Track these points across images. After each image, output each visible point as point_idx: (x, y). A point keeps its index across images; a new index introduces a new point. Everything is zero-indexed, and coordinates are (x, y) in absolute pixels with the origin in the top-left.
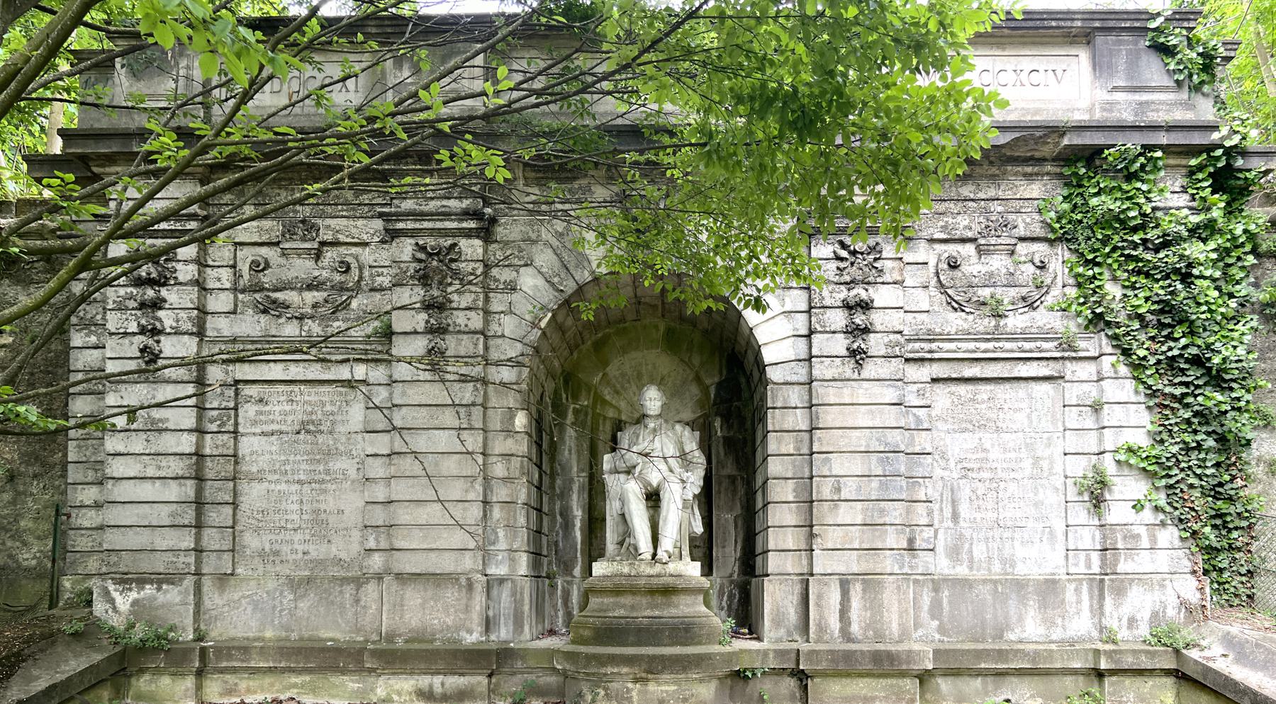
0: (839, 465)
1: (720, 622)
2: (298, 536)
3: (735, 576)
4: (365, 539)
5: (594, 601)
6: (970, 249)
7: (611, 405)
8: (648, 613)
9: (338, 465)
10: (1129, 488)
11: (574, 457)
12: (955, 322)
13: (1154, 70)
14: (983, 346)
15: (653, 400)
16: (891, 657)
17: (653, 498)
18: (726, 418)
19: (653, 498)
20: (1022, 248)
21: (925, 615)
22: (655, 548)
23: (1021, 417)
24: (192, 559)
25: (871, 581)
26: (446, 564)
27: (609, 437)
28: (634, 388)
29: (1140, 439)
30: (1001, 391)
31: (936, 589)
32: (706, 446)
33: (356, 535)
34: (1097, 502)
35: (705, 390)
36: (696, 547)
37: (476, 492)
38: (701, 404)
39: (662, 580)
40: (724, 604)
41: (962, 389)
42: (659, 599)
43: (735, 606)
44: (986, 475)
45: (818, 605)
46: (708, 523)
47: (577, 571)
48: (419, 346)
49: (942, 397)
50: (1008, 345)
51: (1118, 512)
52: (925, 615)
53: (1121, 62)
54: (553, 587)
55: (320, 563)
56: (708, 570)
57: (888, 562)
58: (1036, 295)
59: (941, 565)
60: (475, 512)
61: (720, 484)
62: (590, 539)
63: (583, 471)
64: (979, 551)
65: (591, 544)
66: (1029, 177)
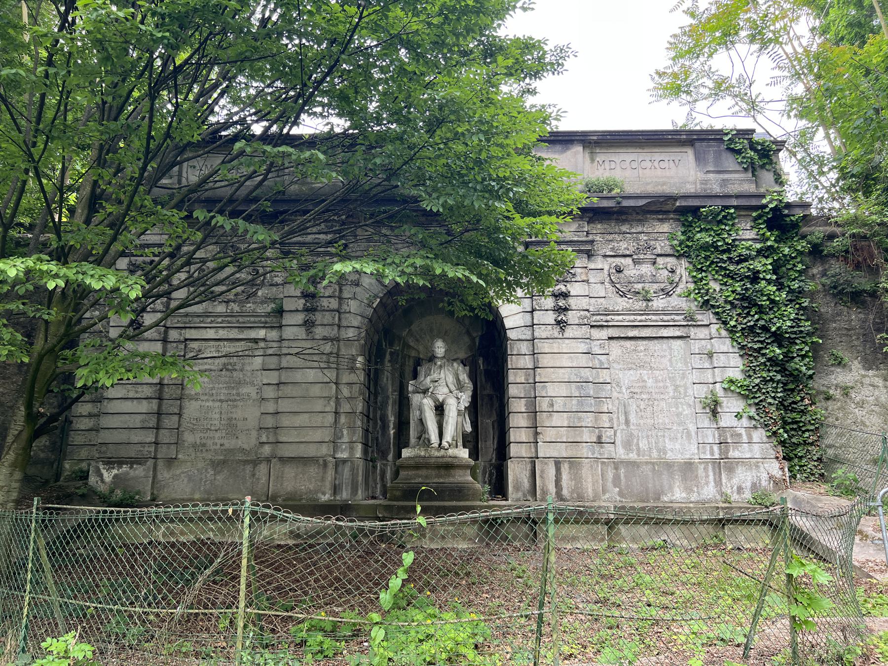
1: (482, 487)
2: (218, 435)
3: (494, 461)
5: (403, 473)
6: (629, 261)
7: (414, 349)
8: (436, 480)
9: (244, 390)
10: (732, 405)
11: (390, 382)
12: (622, 303)
13: (730, 162)
14: (639, 318)
15: (440, 348)
17: (440, 409)
18: (486, 360)
19: (440, 409)
20: (660, 260)
21: (610, 485)
22: (441, 440)
23: (665, 361)
24: (152, 449)
25: (574, 462)
26: (311, 451)
28: (428, 337)
30: (654, 345)
31: (616, 468)
32: (473, 376)
33: (254, 434)
34: (714, 413)
36: (468, 441)
39: (445, 460)
40: (486, 479)
41: (628, 344)
42: (443, 472)
43: (493, 481)
44: (644, 396)
45: (541, 477)
46: (475, 424)
47: (390, 457)
48: (300, 318)
49: (616, 349)
50: (654, 318)
51: (727, 420)
52: (610, 485)
53: (711, 157)
54: (375, 467)
55: (231, 451)
56: (474, 454)
57: (585, 450)
58: (669, 288)
59: (620, 453)
60: (330, 418)
61: (482, 400)
62: (399, 436)
63: (395, 391)
64: (643, 444)
65: (399, 439)
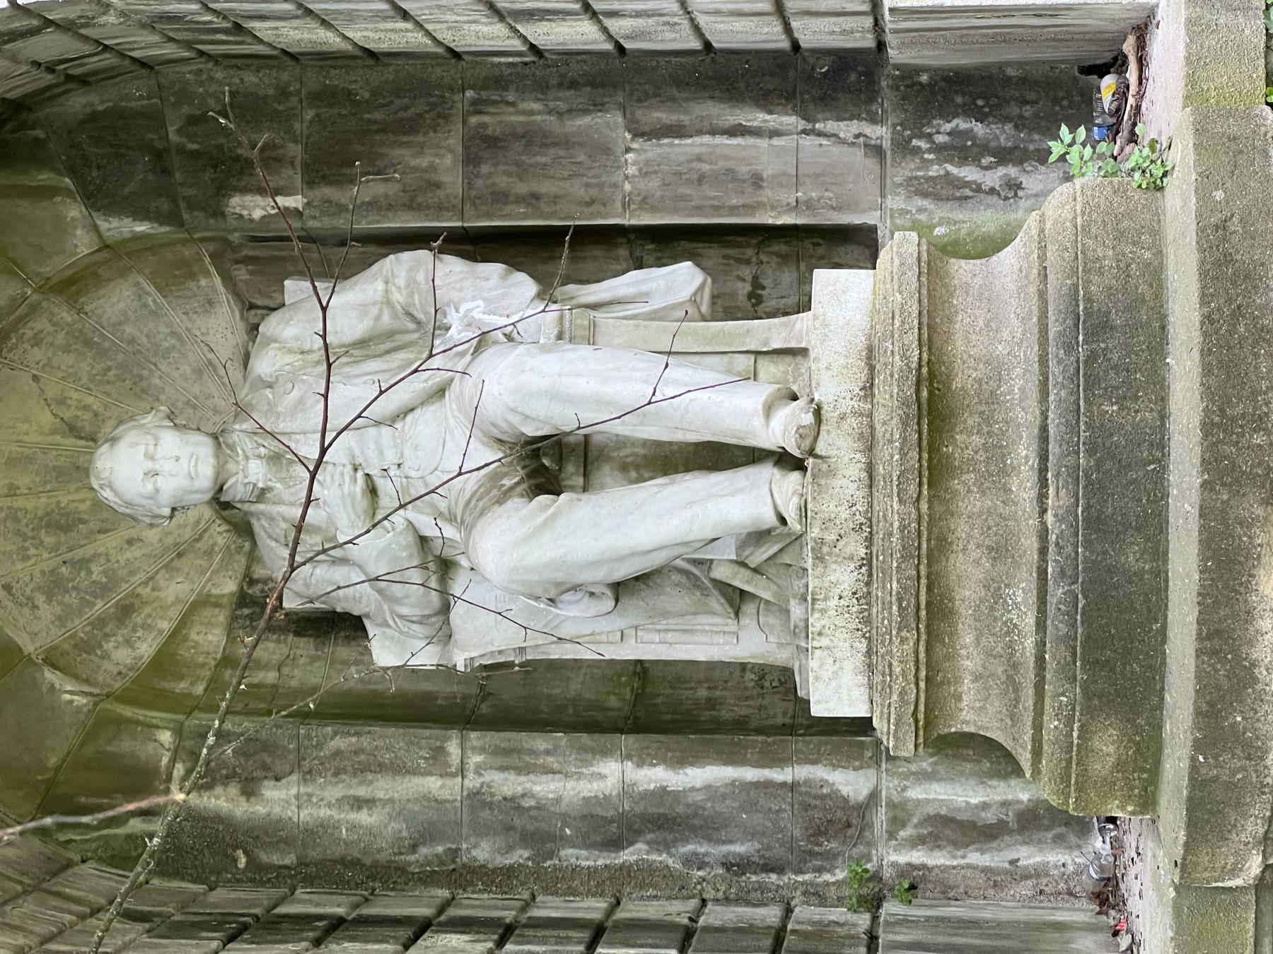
3: (880, 133)
15: (151, 466)
17: (550, 463)
27: (305, 647)
32: (342, 253)
35: (116, 258)
38: (174, 276)
40: (992, 178)
43: (1004, 134)
47: (851, 782)
61: (500, 198)
62: (718, 727)
63: (439, 753)
65: (740, 726)
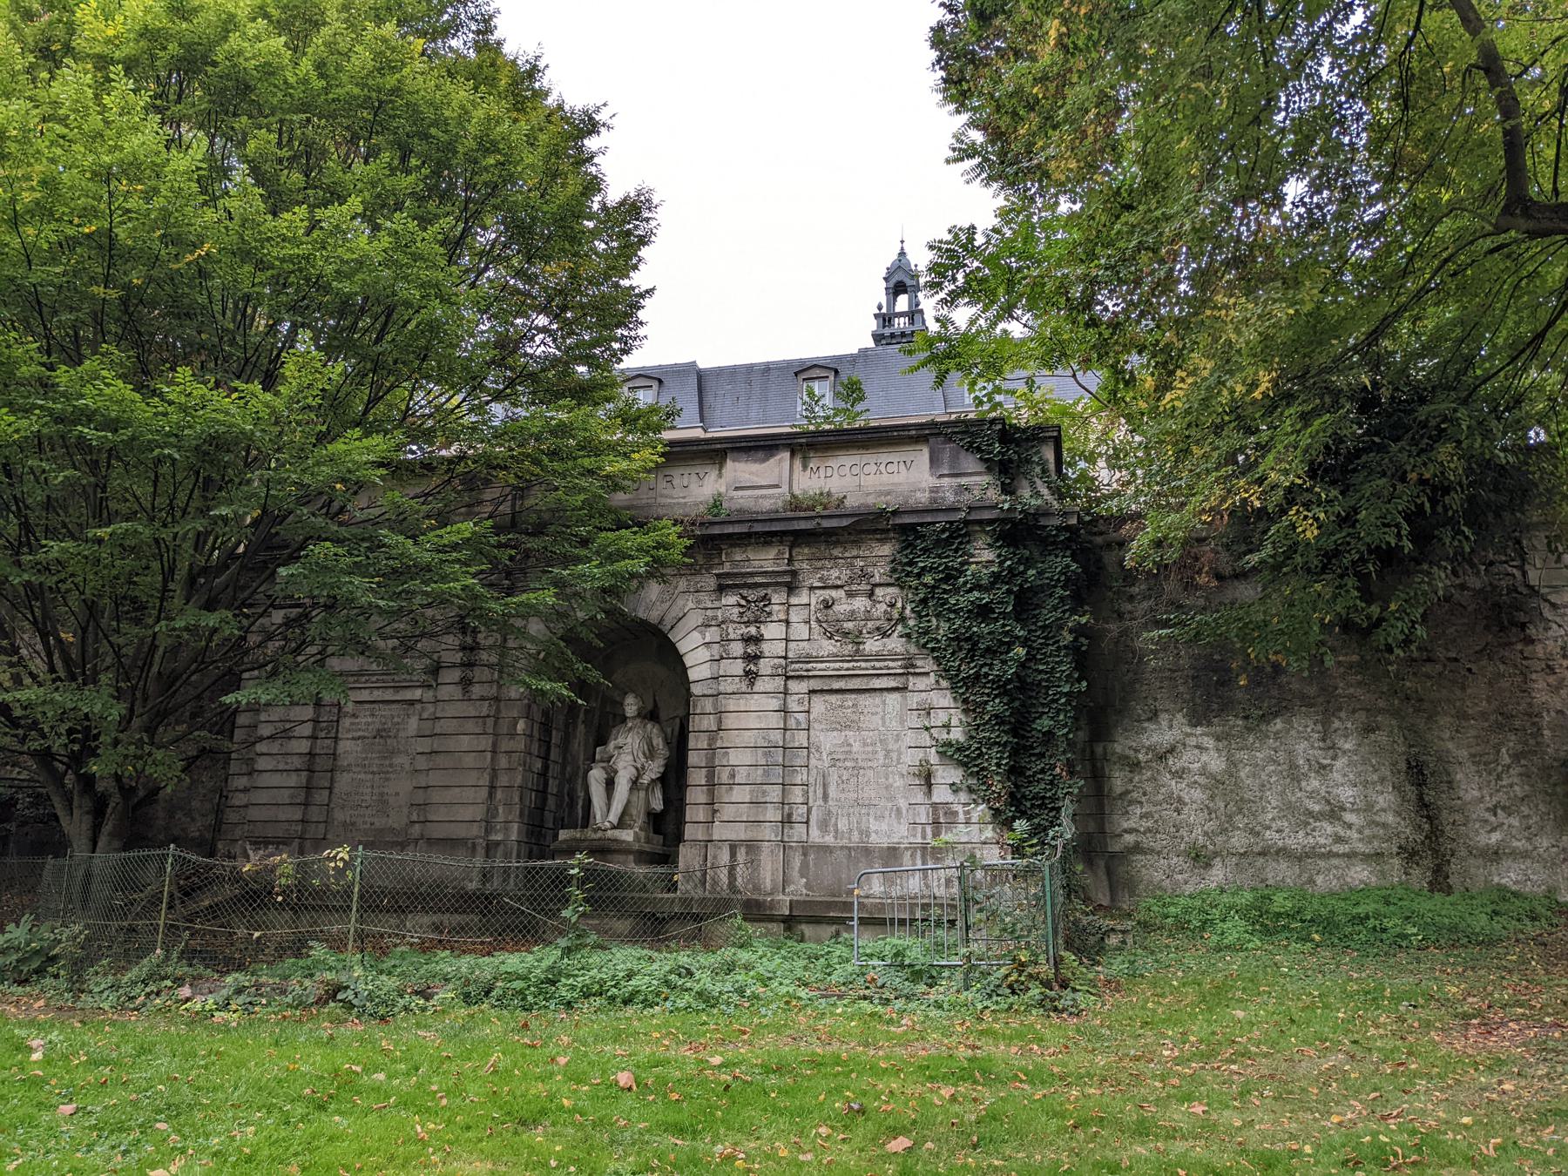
0: (734, 758)
2: (369, 812)
4: (410, 813)
6: (841, 593)
9: (398, 760)
10: (948, 775)
12: (828, 647)
13: (970, 463)
14: (846, 665)
16: (758, 904)
19: (610, 784)
20: (879, 592)
21: (796, 874)
23: (877, 720)
24: (299, 828)
25: (752, 846)
26: (460, 832)
29: (957, 735)
30: (865, 701)
31: (805, 854)
33: (405, 810)
34: (929, 785)
37: (485, 780)
41: (833, 698)
44: (848, 764)
48: (456, 675)
49: (819, 705)
50: (863, 665)
51: (941, 794)
52: (796, 874)
53: (946, 456)
55: (381, 830)
57: (767, 831)
58: (886, 626)
59: (816, 836)
60: (484, 793)
64: (842, 825)
66: (882, 541)
